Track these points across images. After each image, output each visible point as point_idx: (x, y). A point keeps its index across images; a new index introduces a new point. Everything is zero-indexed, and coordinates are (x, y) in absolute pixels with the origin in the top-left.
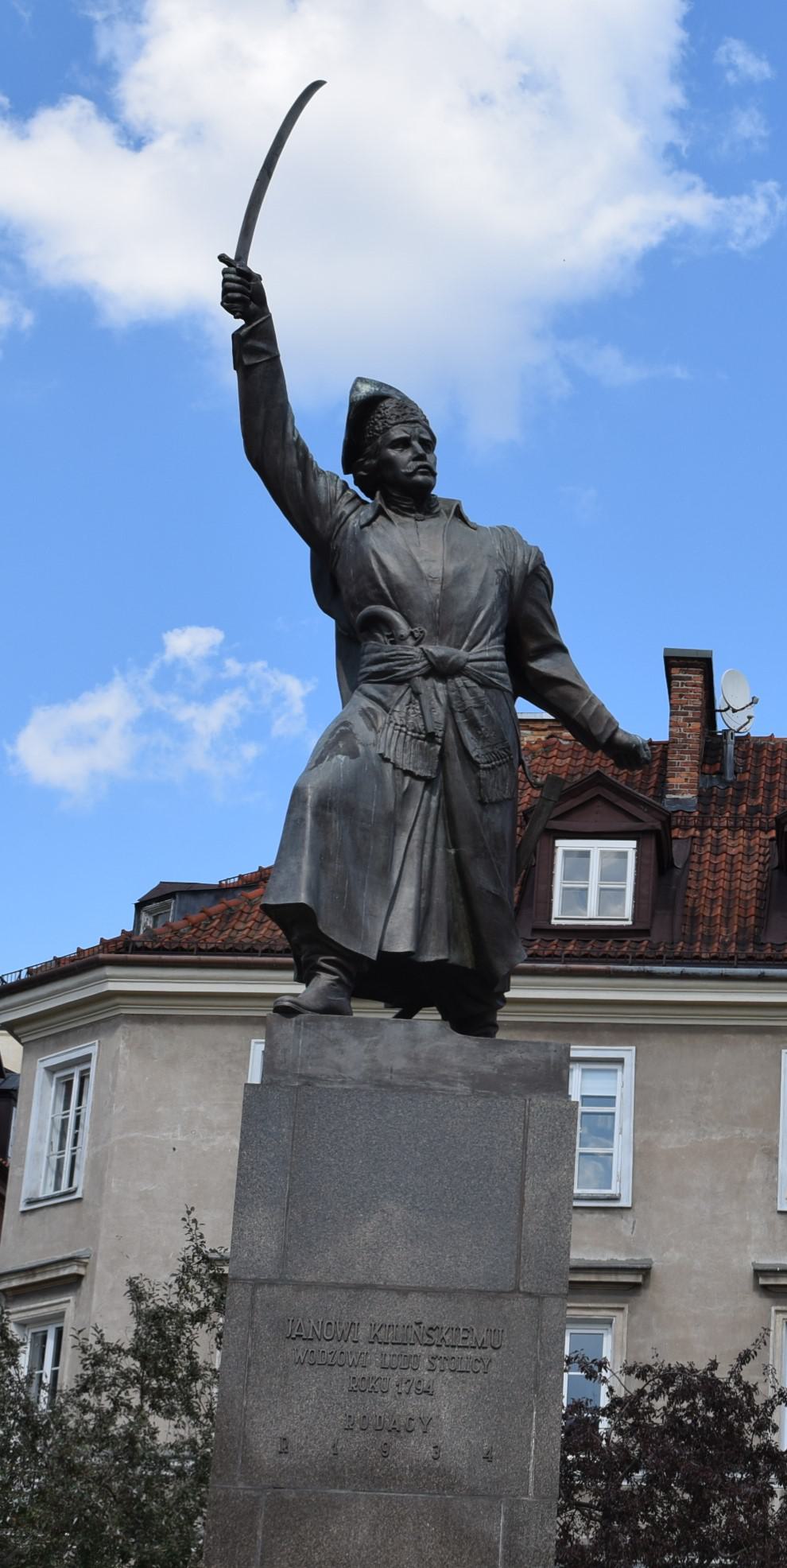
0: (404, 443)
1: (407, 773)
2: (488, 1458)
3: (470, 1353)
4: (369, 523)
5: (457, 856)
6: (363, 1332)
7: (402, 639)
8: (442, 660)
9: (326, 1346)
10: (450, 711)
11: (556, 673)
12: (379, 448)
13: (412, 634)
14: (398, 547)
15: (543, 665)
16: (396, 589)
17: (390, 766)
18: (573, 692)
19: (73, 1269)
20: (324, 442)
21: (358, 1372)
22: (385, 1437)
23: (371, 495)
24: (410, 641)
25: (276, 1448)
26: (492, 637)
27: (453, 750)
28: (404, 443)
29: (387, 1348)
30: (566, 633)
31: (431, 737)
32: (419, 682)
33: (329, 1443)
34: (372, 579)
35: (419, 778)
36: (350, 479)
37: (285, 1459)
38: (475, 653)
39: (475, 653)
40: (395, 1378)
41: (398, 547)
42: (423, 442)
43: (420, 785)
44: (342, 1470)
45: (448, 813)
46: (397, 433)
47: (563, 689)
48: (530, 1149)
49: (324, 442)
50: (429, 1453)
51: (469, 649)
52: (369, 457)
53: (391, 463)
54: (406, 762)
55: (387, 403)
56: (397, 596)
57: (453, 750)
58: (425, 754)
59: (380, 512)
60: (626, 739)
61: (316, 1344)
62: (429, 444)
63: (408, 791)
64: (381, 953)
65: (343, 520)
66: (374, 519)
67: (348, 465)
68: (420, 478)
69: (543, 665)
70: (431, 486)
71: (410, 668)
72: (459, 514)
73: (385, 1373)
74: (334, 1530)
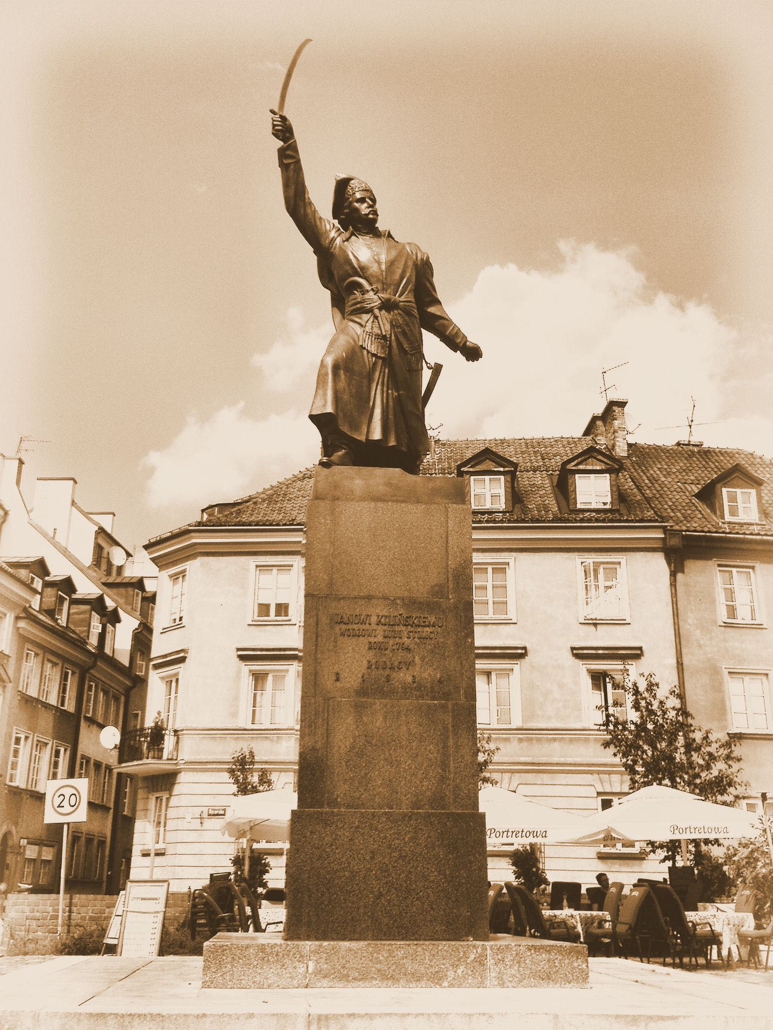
0: (362, 200)
1: (373, 355)
2: (440, 682)
3: (427, 629)
4: (347, 240)
5: (399, 395)
6: (374, 619)
7: (368, 291)
8: (388, 300)
9: (355, 627)
10: (392, 326)
11: (438, 313)
12: (351, 203)
13: (372, 289)
14: (361, 251)
15: (432, 310)
16: (363, 269)
17: (365, 352)
18: (445, 322)
19: (182, 655)
20: (322, 200)
21: (372, 640)
22: (387, 672)
23: (346, 229)
24: (371, 293)
25: (334, 678)
26: (409, 292)
27: (394, 344)
28: (362, 200)
29: (386, 627)
30: (440, 296)
31: (384, 337)
32: (376, 311)
33: (360, 675)
34: (351, 264)
35: (380, 358)
36: (336, 222)
37: (338, 684)
38: (402, 298)
39: (402, 298)
40: (391, 642)
41: (361, 251)
42: (371, 199)
43: (380, 362)
44: (367, 689)
45: (393, 376)
46: (358, 195)
47: (442, 321)
48: (450, 528)
49: (322, 200)
50: (410, 679)
51: (400, 296)
52: (346, 208)
53: (357, 210)
54: (373, 349)
55: (352, 182)
56: (362, 271)
57: (394, 344)
58: (383, 347)
59: (352, 234)
60: (471, 345)
61: (350, 626)
62: (374, 200)
63: (375, 364)
64: (367, 439)
65: (333, 240)
66: (349, 238)
67: (335, 215)
68: (371, 216)
69: (432, 310)
70: (375, 221)
71: (372, 305)
72: (390, 236)
73: (386, 640)
74: (365, 719)
